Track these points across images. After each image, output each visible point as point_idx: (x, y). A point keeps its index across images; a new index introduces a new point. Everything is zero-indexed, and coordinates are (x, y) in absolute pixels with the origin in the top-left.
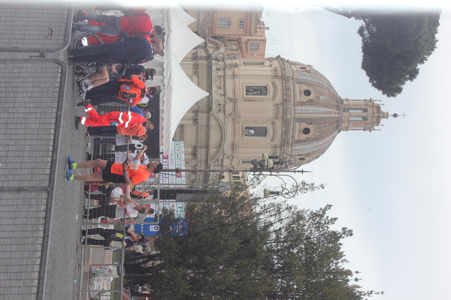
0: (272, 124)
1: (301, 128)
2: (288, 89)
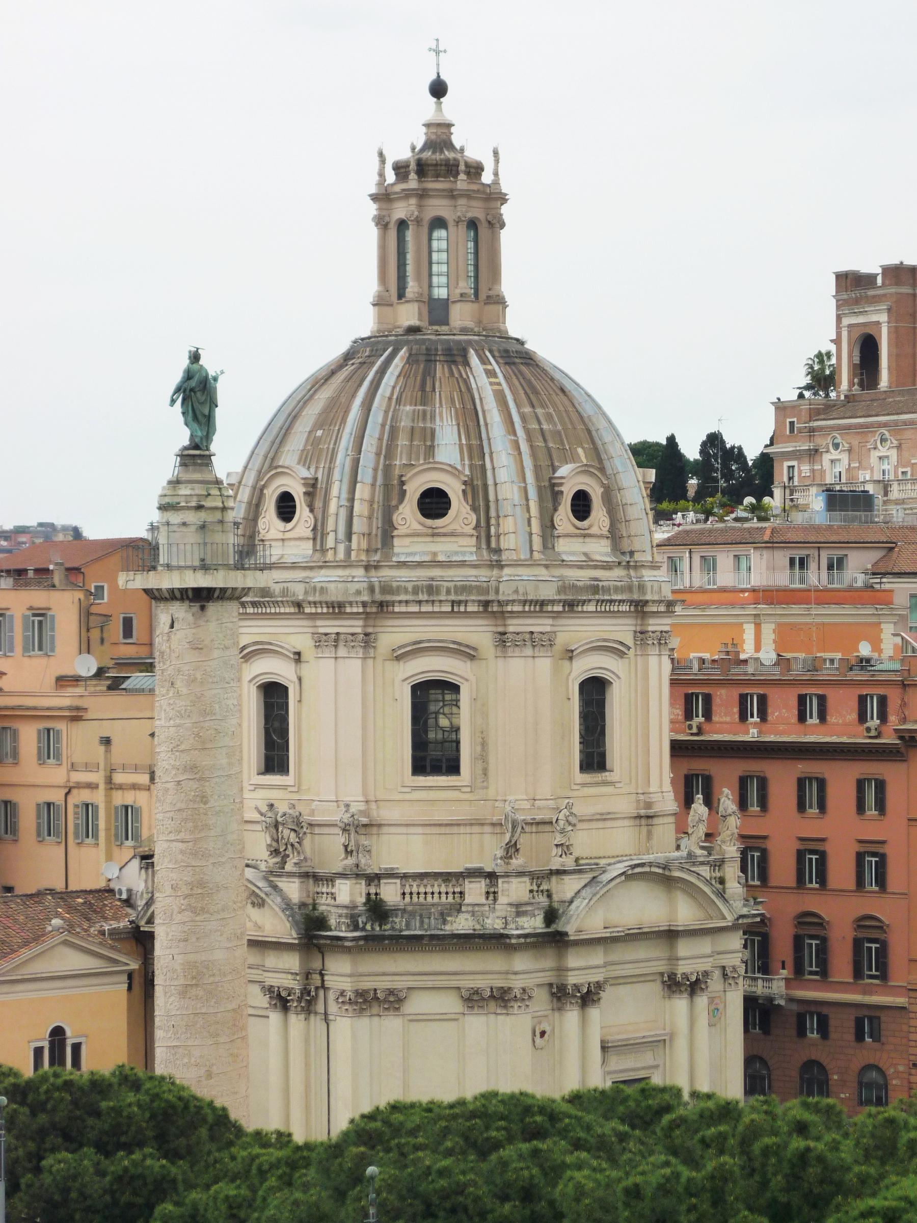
0: (571, 658)
2: (431, 590)
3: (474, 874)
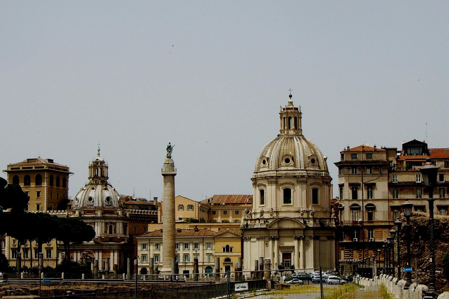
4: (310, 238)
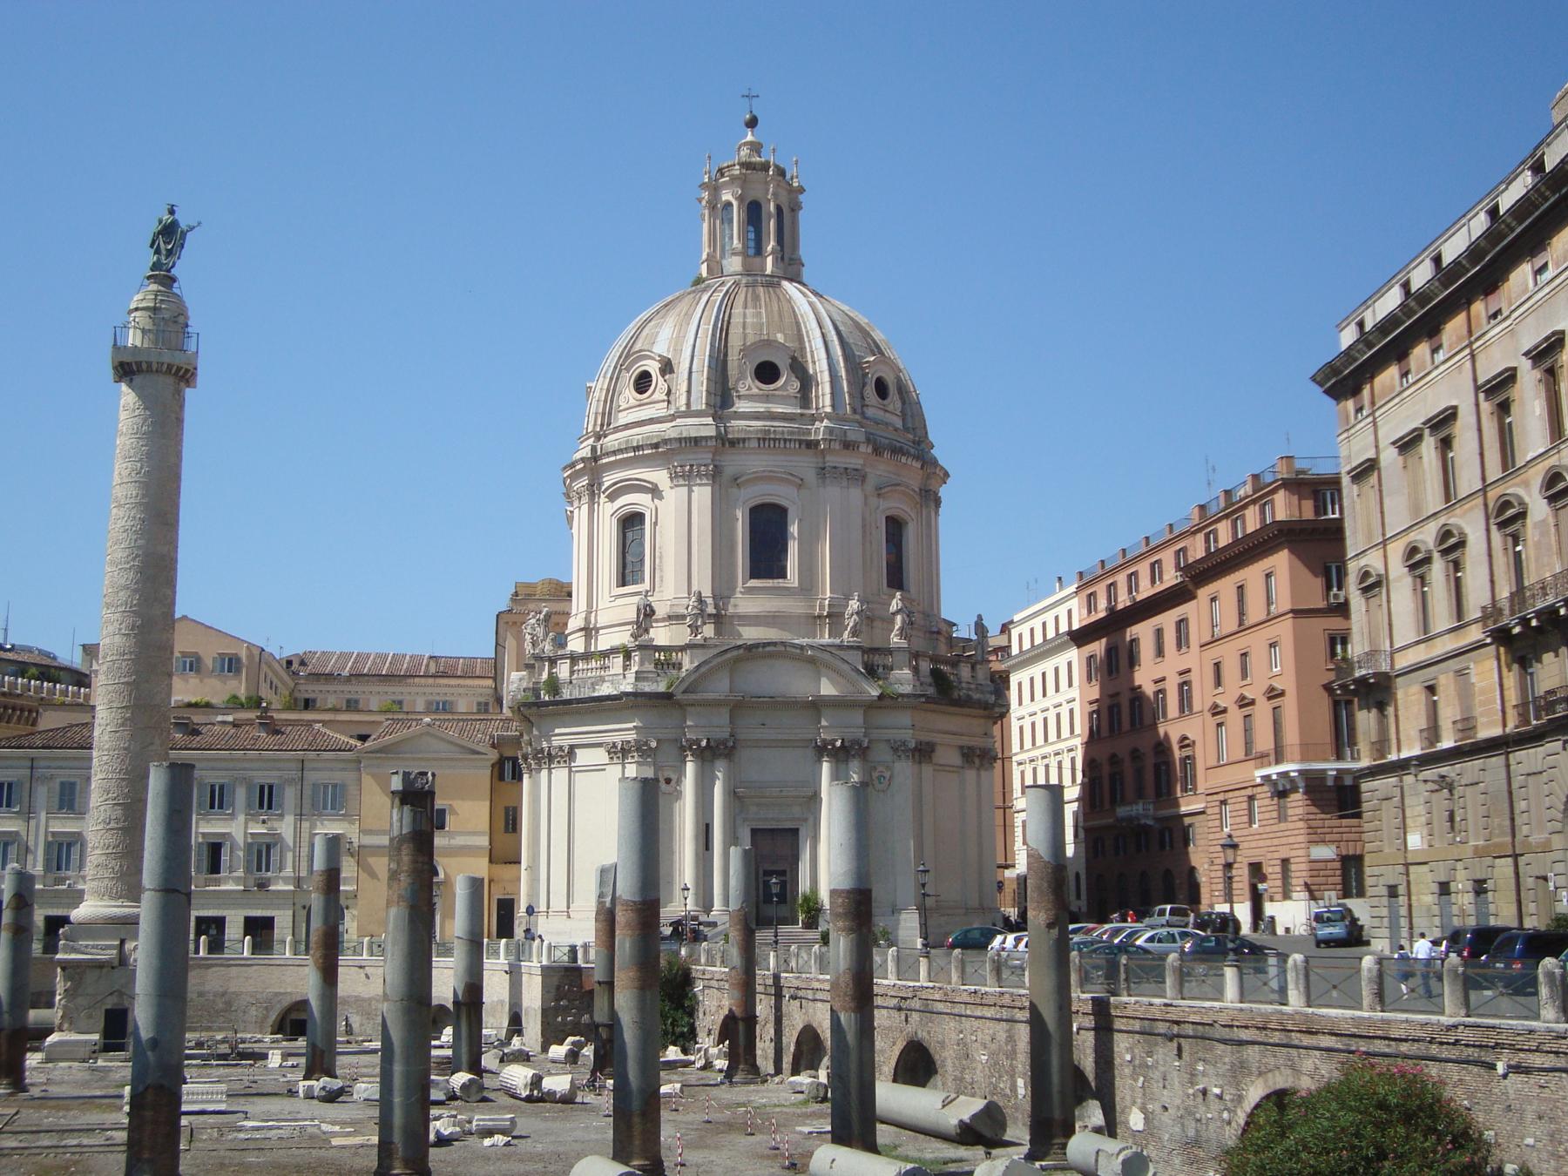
1: (755, 391)
3: (613, 651)
4: (895, 750)
